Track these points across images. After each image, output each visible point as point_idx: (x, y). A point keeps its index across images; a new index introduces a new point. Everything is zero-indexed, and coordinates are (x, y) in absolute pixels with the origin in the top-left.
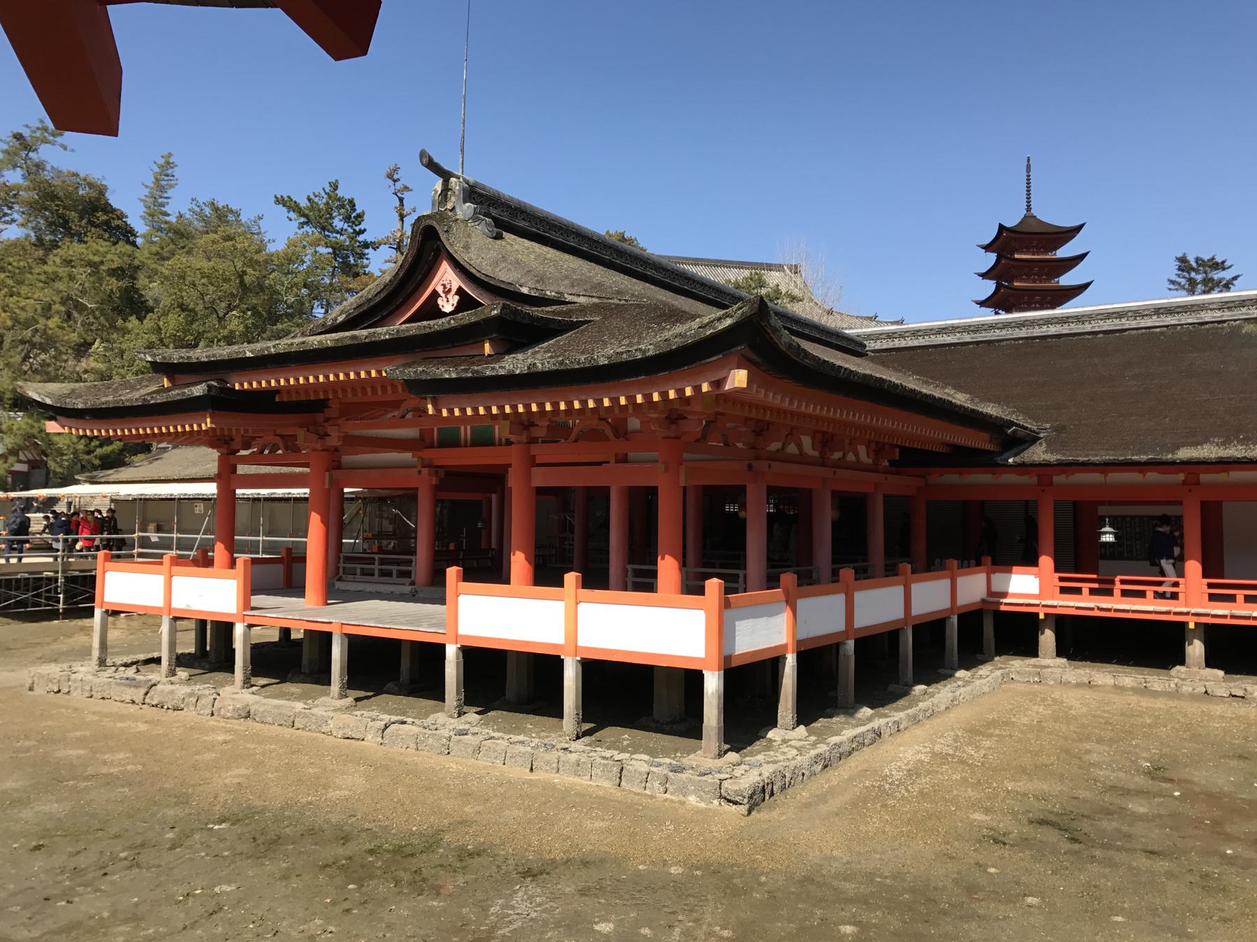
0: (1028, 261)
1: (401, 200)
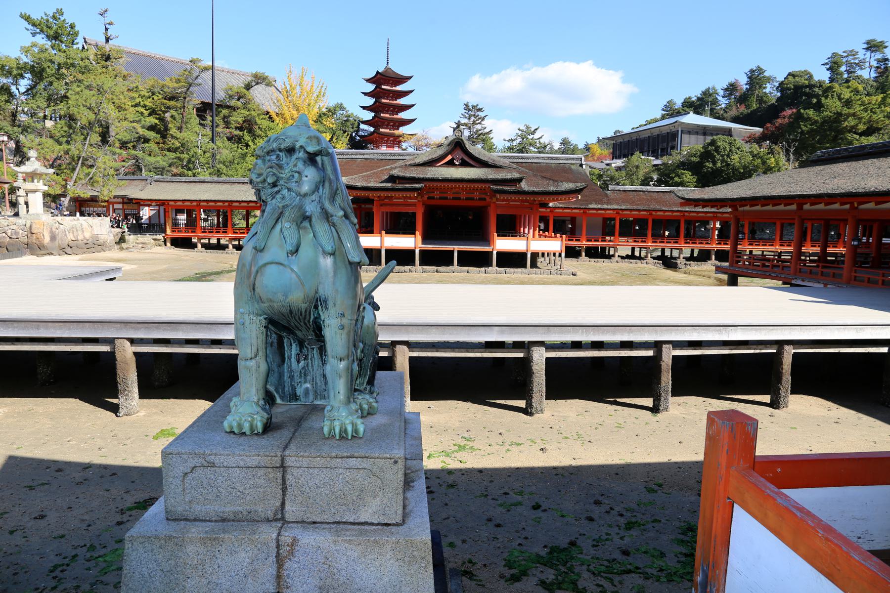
0: (387, 89)
1: (106, 29)
